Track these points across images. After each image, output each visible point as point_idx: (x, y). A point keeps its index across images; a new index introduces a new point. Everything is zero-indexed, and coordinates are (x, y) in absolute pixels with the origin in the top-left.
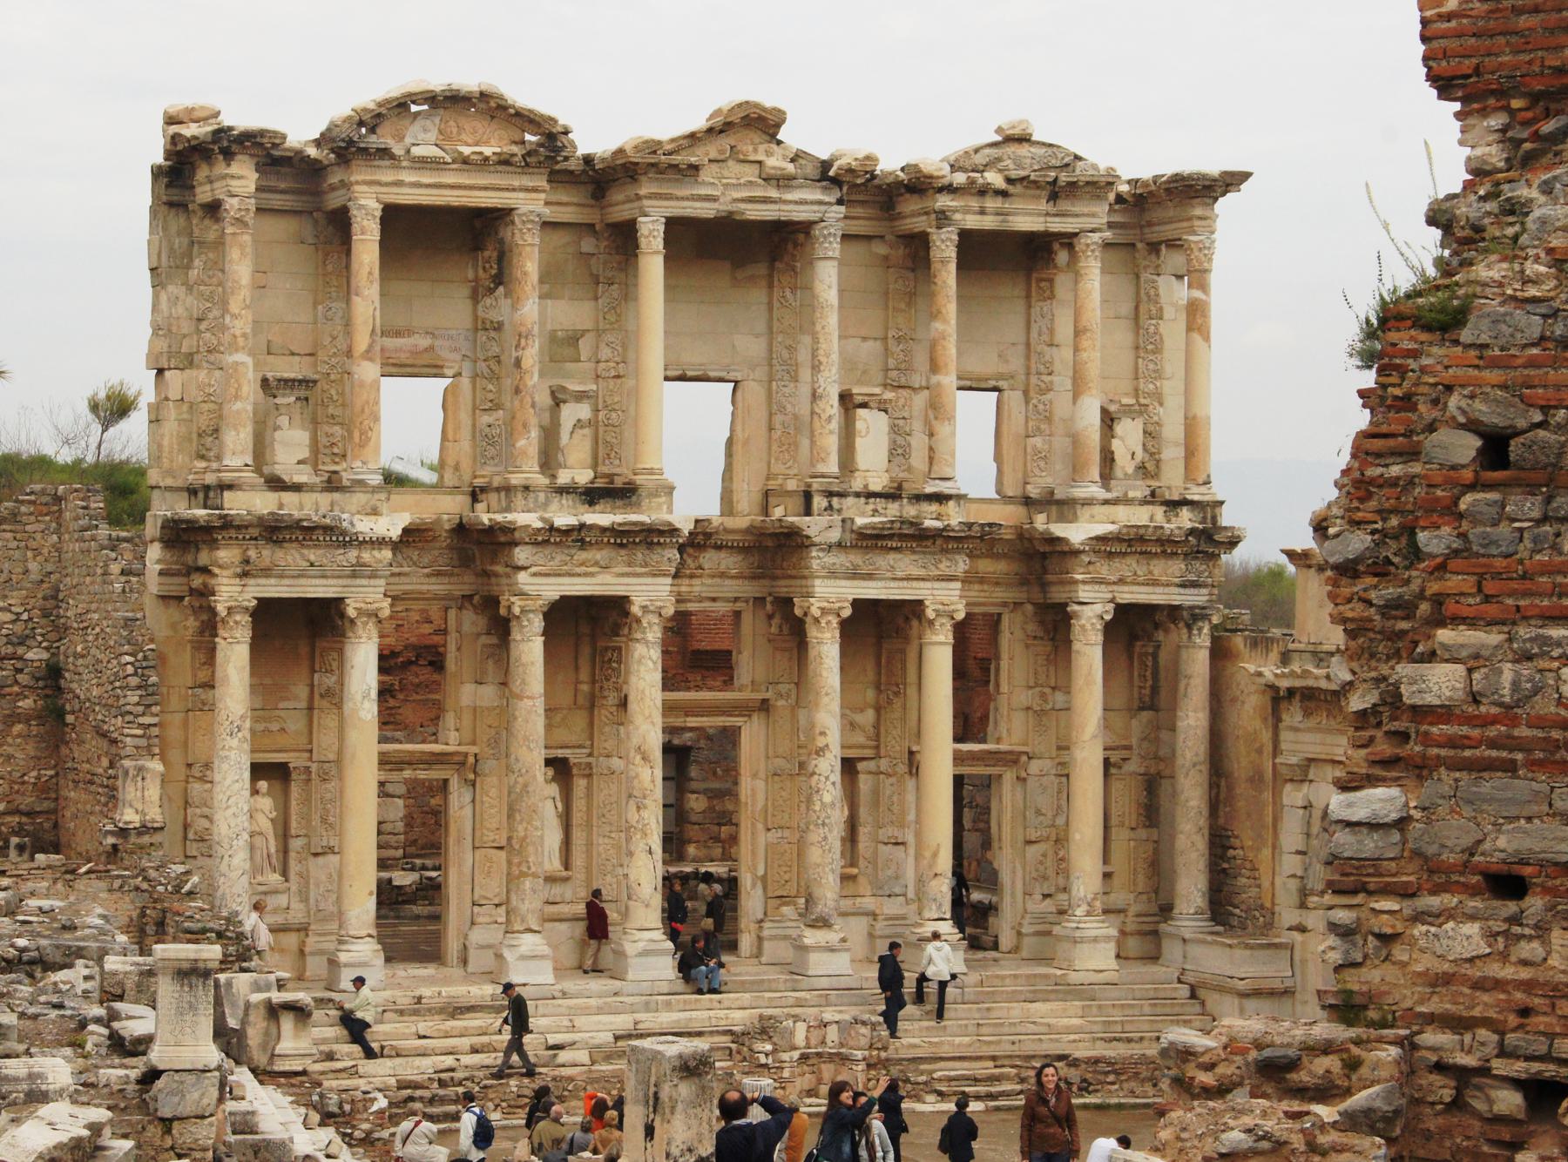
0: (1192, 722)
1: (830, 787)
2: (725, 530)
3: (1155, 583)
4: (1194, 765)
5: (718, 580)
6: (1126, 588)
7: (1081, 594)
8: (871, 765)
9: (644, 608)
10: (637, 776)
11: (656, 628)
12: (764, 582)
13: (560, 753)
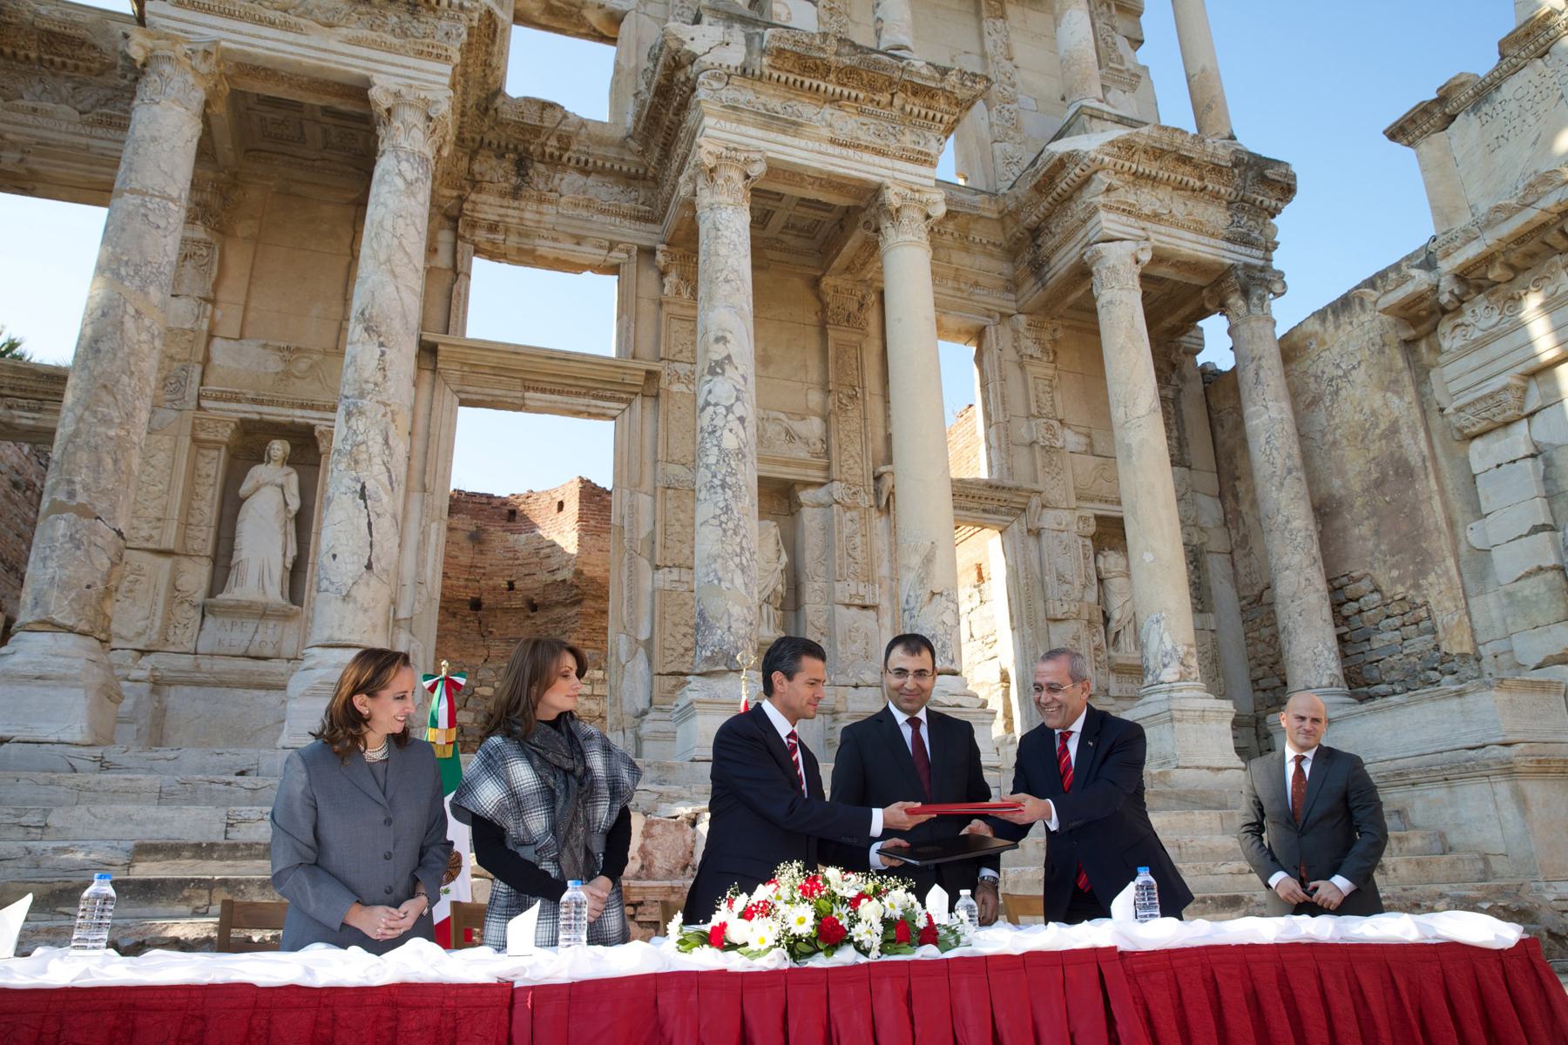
0: (1274, 414)
1: (736, 425)
2: (589, 137)
3: (1199, 229)
4: (1290, 472)
5: (584, 213)
6: (1162, 229)
7: (1104, 224)
8: (820, 494)
9: (397, 95)
10: (354, 358)
11: (417, 134)
12: (651, 227)
13: (299, 416)
